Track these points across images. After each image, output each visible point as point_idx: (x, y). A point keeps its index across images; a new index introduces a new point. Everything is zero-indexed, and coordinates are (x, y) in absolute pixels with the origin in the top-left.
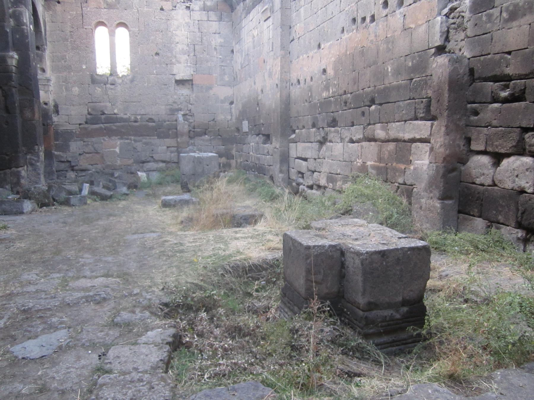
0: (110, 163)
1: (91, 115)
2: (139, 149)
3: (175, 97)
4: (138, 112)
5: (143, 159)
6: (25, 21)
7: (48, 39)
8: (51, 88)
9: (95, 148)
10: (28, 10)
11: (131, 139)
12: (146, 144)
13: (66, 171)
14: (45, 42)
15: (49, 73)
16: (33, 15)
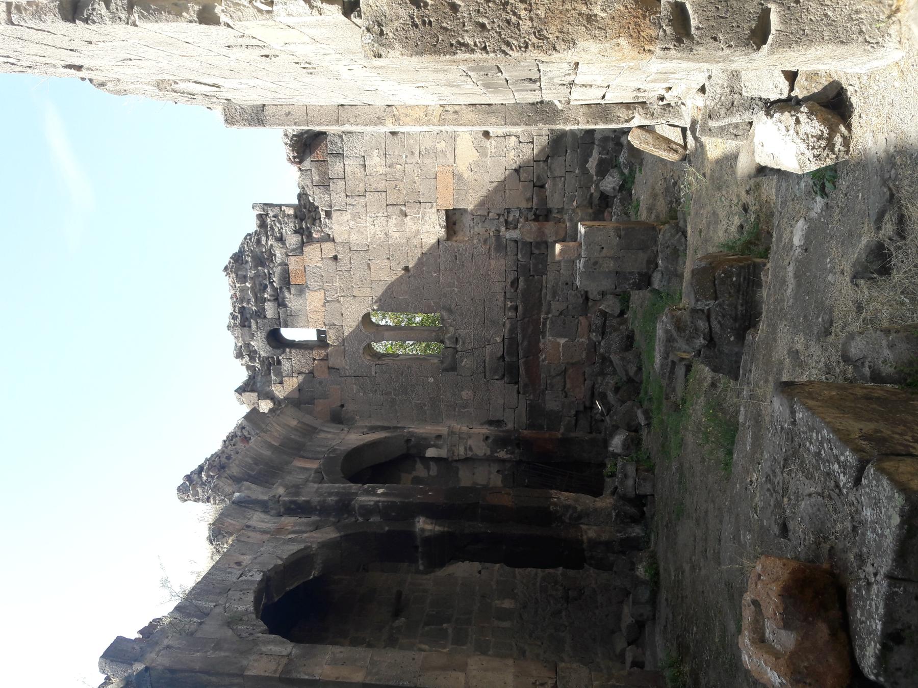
0: (584, 353)
1: (504, 375)
2: (562, 307)
3: (475, 241)
4: (501, 304)
5: (581, 301)
6: (372, 503)
7: (394, 423)
8: (465, 429)
9: (558, 375)
10: (356, 494)
11: (546, 319)
12: (554, 294)
13: (591, 417)
14: (398, 433)
15: (443, 430)
16: (364, 484)
